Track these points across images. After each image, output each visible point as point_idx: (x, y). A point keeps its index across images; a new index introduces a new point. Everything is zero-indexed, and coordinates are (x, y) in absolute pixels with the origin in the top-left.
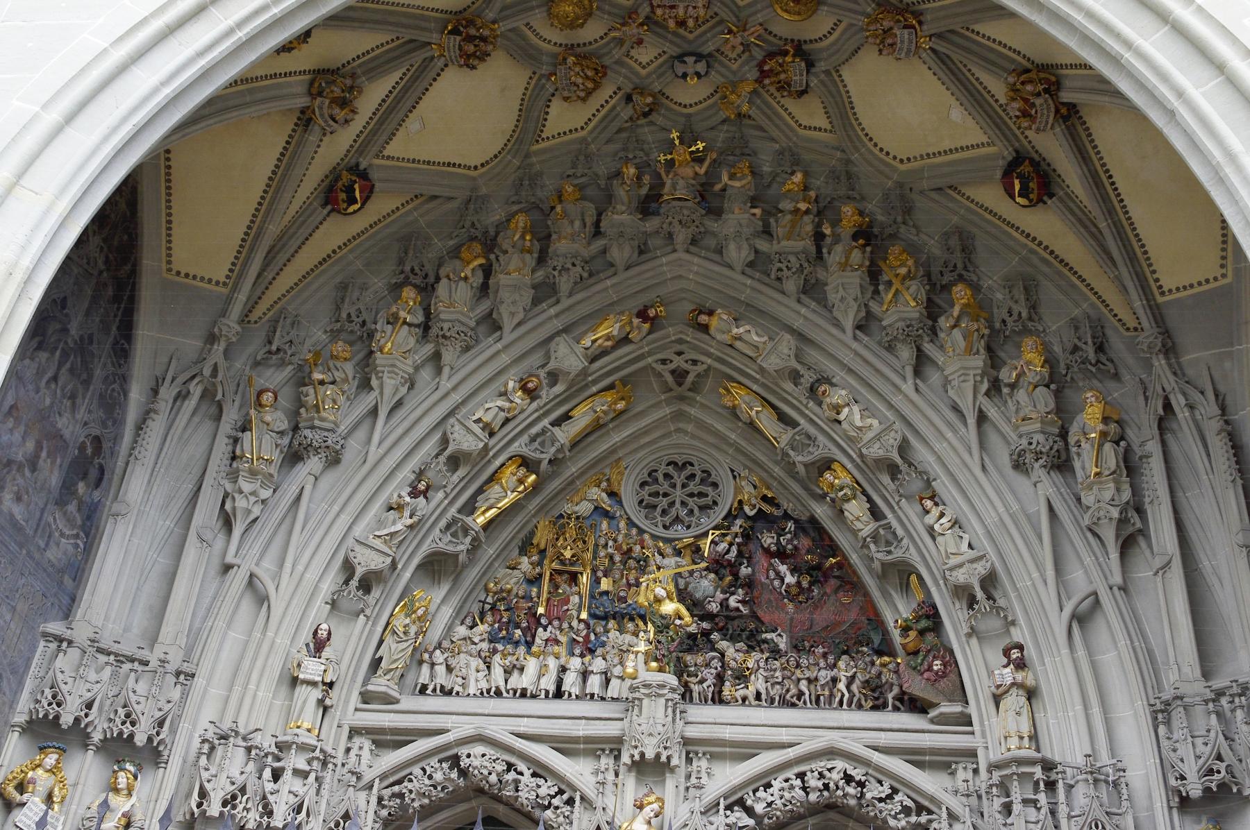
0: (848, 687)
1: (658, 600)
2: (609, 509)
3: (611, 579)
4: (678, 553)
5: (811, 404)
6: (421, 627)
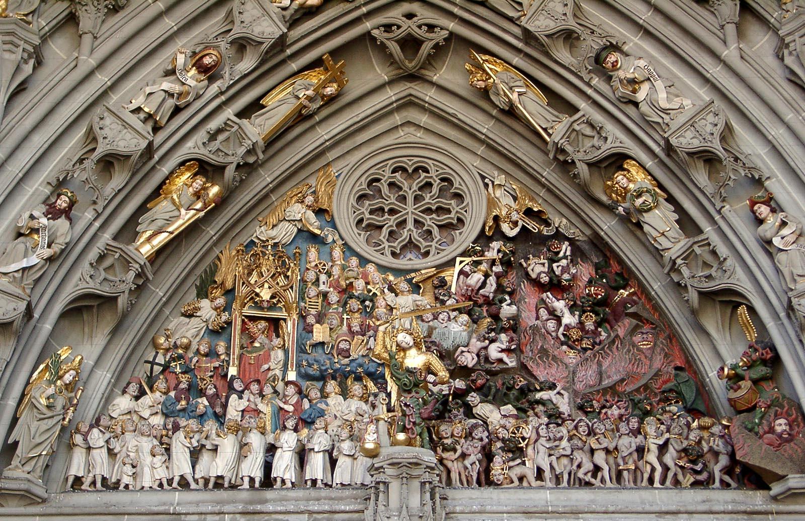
0: (660, 458)
1: (402, 349)
2: (317, 232)
3: (326, 326)
4: (416, 288)
5: (595, 81)
6: (70, 399)
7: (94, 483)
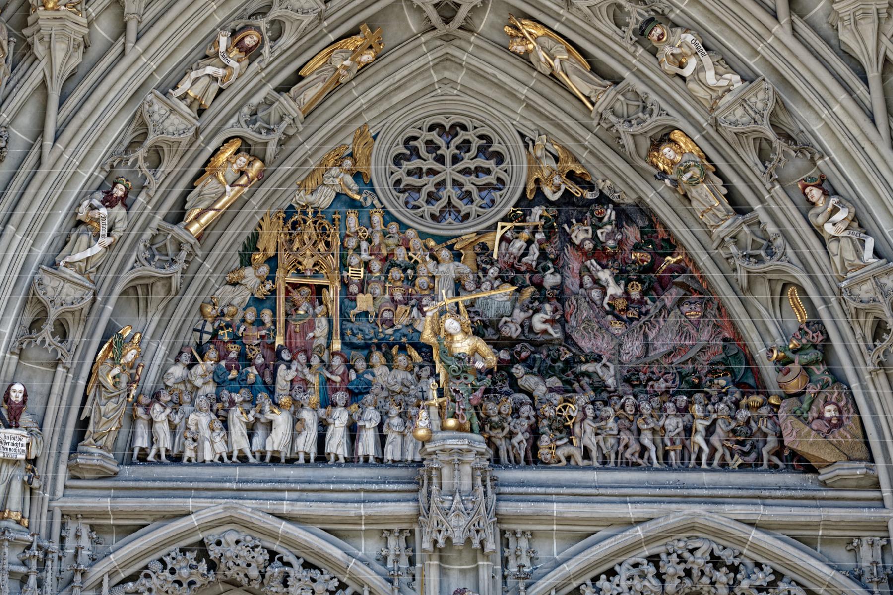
2: (357, 197)
3: (369, 295)
7: (158, 455)
